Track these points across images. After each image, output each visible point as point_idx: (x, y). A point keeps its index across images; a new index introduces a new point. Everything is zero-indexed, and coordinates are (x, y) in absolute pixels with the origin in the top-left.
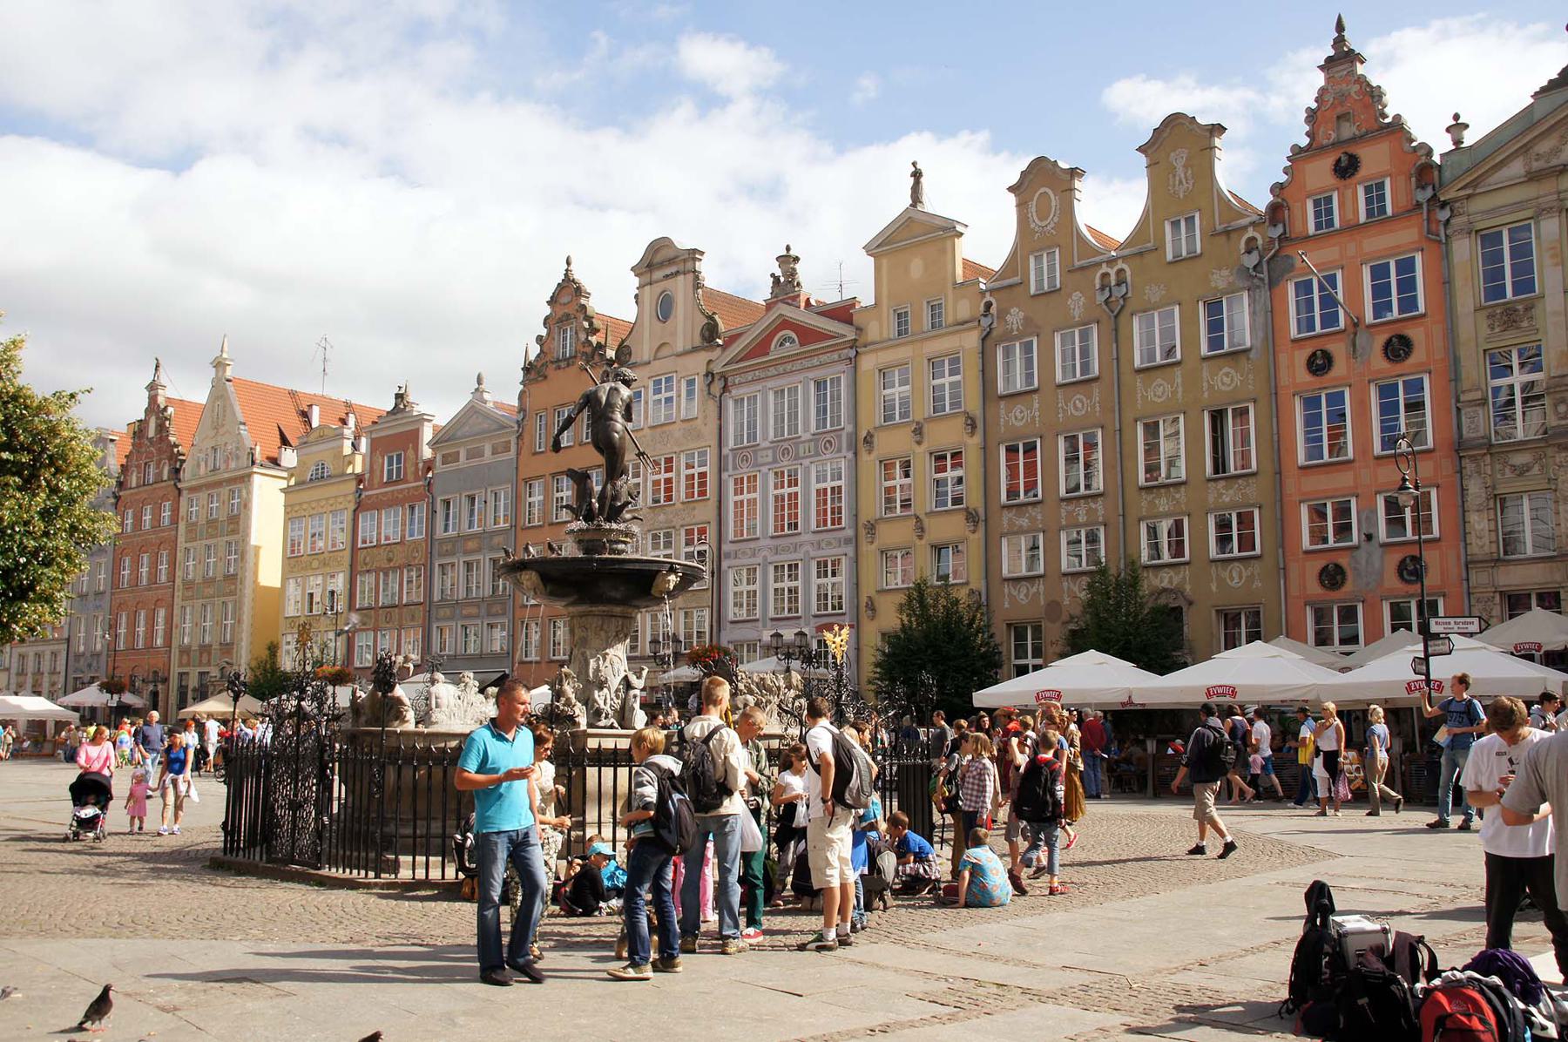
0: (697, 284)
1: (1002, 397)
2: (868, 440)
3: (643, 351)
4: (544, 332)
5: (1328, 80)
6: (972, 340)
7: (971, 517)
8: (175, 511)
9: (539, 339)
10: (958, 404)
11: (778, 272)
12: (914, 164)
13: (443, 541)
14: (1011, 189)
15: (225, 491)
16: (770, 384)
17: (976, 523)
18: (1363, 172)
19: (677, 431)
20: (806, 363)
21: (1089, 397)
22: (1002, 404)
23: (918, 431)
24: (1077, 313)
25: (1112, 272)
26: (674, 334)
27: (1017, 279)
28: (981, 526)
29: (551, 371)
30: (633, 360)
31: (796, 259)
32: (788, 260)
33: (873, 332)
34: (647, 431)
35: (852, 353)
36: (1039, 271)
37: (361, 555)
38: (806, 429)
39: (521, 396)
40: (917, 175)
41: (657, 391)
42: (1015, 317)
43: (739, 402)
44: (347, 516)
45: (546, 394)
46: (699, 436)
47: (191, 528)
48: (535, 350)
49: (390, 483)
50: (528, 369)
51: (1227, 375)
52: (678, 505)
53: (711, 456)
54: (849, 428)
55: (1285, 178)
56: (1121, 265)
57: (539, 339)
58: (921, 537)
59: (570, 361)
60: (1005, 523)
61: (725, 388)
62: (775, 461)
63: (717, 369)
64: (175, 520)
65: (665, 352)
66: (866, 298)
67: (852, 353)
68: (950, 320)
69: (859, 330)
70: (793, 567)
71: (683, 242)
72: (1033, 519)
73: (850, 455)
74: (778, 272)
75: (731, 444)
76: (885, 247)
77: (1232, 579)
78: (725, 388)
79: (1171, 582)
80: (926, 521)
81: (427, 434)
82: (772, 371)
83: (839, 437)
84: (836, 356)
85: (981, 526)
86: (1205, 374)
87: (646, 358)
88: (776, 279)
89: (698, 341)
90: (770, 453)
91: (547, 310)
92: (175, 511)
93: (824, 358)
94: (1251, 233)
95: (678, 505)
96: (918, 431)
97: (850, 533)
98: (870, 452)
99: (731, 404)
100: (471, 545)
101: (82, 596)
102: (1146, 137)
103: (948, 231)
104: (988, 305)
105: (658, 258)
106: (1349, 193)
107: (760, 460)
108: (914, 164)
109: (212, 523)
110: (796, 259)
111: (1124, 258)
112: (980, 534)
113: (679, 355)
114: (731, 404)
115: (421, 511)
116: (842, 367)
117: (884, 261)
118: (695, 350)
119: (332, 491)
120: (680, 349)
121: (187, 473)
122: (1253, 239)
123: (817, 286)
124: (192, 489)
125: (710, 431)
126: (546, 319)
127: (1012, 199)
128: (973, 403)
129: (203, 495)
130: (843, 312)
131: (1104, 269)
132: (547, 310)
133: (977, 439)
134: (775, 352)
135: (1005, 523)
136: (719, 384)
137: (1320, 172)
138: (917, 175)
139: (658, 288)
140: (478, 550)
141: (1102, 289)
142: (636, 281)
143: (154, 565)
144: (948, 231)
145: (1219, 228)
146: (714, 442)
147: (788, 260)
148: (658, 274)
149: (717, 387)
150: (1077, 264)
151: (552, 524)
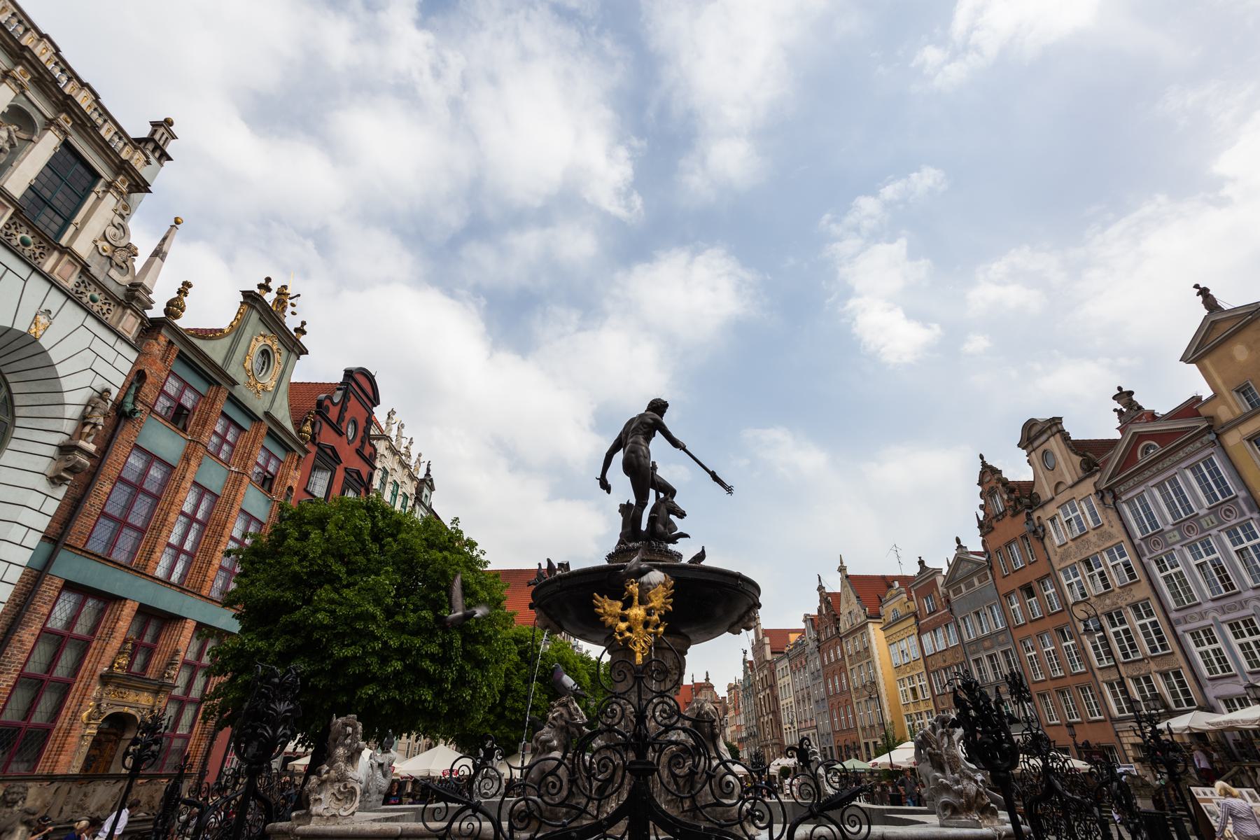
0: (1066, 437)
3: (1046, 491)
4: (982, 502)
8: (842, 649)
9: (981, 507)
11: (1119, 407)
15: (859, 635)
16: (1150, 483)
19: (1092, 537)
20: (1174, 458)
26: (1062, 474)
29: (994, 523)
30: (1043, 499)
32: (1124, 396)
34: (1070, 543)
37: (929, 660)
38: (1201, 506)
39: (983, 542)
41: (1066, 514)
43: (1129, 502)
45: (997, 540)
46: (1111, 536)
48: (981, 514)
49: (931, 613)
52: (1117, 590)
53: (1127, 548)
57: (981, 507)
59: (1003, 514)
61: (1115, 498)
62: (1183, 538)
63: (1103, 486)
65: (1062, 488)
71: (1043, 415)
74: (1119, 407)
75: (1139, 535)
78: (1115, 498)
81: (940, 580)
82: (1147, 474)
83: (1237, 504)
87: (1050, 496)
88: (1120, 412)
89: (1081, 474)
90: (1176, 533)
91: (980, 489)
92: (842, 649)
93: (1188, 449)
95: (1117, 590)
99: (1125, 507)
100: (987, 644)
105: (1033, 433)
107: (1170, 541)
113: (1072, 487)
114: (1125, 507)
115: (952, 629)
118: (1080, 481)
119: (904, 625)
120: (1070, 482)
121: (842, 630)
124: (846, 636)
125: (1117, 531)
126: (981, 495)
129: (851, 639)
130: (1191, 408)
132: (980, 489)
134: (1142, 459)
136: (1109, 495)
139: (1040, 451)
140: (992, 647)
142: (1025, 452)
143: (840, 680)
146: (1124, 537)
147: (1124, 396)
148: (1036, 444)
151: (1032, 621)
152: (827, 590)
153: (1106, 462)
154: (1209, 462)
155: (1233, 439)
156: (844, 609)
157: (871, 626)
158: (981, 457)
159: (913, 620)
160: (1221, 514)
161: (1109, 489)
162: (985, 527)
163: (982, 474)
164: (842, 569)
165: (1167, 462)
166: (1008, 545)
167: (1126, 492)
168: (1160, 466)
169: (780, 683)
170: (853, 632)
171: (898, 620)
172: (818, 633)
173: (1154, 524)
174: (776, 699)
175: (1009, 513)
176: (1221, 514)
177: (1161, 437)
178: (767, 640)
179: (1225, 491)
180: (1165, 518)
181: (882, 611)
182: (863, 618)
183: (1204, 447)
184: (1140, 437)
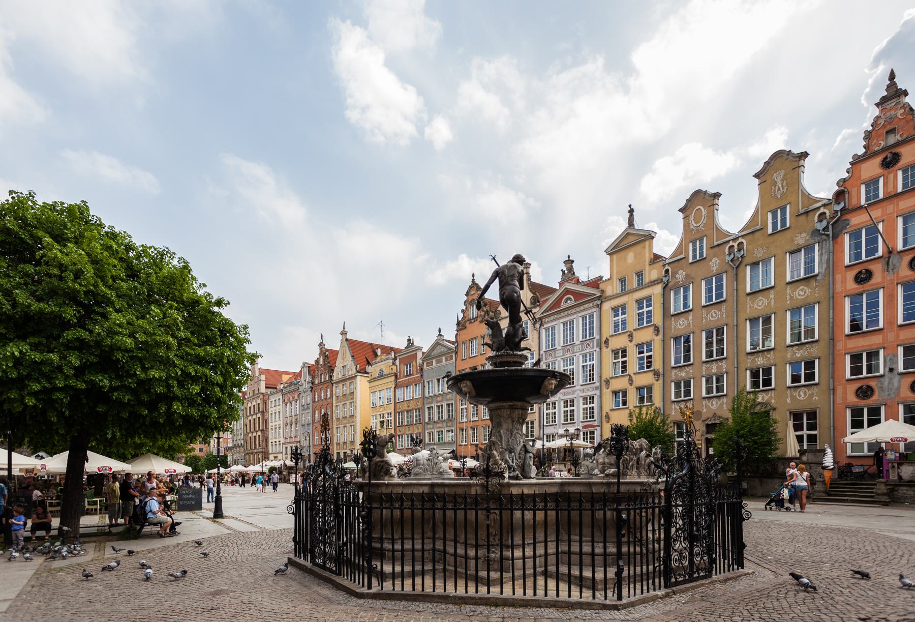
1: (673, 315)
2: (607, 342)
5: (881, 111)
6: (658, 289)
7: (656, 374)
8: (331, 392)
9: (463, 311)
10: (651, 321)
11: (565, 269)
12: (630, 206)
13: (428, 398)
14: (681, 210)
15: (348, 383)
17: (659, 376)
18: (903, 162)
20: (578, 309)
21: (720, 310)
22: (673, 319)
23: (631, 336)
24: (714, 269)
25: (736, 245)
27: (683, 256)
28: (661, 377)
29: (467, 325)
31: (573, 262)
33: (609, 291)
35: (599, 302)
36: (694, 250)
37: (398, 405)
40: (631, 211)
42: (681, 275)
43: (547, 329)
44: (393, 389)
45: (466, 335)
47: (337, 397)
48: (461, 316)
50: (458, 324)
51: (802, 290)
54: (598, 337)
55: (847, 175)
56: (740, 240)
57: (463, 311)
58: (631, 385)
60: (673, 374)
61: (541, 325)
64: (331, 397)
66: (606, 276)
67: (599, 302)
68: (647, 281)
69: (603, 291)
70: (572, 401)
72: (687, 373)
73: (598, 349)
74: (565, 269)
76: (615, 250)
79: (763, 398)
80: (634, 377)
81: (420, 355)
82: (562, 314)
84: (591, 305)
85: (661, 377)
86: (788, 291)
91: (465, 298)
92: (331, 392)
93: (586, 306)
94: (822, 210)
96: (631, 336)
97: (598, 384)
98: (607, 347)
100: (439, 399)
101: (303, 425)
102: (759, 167)
103: (649, 237)
104: (667, 271)
106: (891, 176)
108: (630, 206)
109: (344, 395)
110: (573, 262)
111: (742, 236)
112: (661, 381)
114: (544, 331)
115: (419, 387)
116: (595, 309)
117: (615, 257)
122: (824, 213)
123: (583, 274)
127: (681, 215)
128: (657, 319)
129: (341, 385)
130: (595, 283)
131: (731, 243)
132: (465, 298)
133: (660, 337)
134: (563, 305)
135: (673, 374)
137: (872, 168)
138: (631, 211)
141: (730, 254)
144: (649, 237)
145: (801, 211)
149: (537, 325)
150: (716, 243)
152: (326, 347)
153: (544, 302)
154: (591, 316)
156: (339, 363)
157: (358, 378)
158: (473, 276)
159: (393, 378)
160: (584, 346)
161: (540, 319)
162: (461, 326)
163: (471, 288)
164: (343, 333)
165: (574, 311)
166: (471, 340)
167: (548, 322)
168: (569, 312)
169: (271, 410)
170: (343, 381)
171: (382, 376)
172: (313, 378)
173: (554, 345)
174: (266, 422)
175: (479, 319)
176: (584, 346)
177: (578, 295)
178: (263, 377)
179: (591, 334)
180: (560, 342)
181: (369, 369)
182: (354, 371)
183: (593, 307)
184: (568, 291)
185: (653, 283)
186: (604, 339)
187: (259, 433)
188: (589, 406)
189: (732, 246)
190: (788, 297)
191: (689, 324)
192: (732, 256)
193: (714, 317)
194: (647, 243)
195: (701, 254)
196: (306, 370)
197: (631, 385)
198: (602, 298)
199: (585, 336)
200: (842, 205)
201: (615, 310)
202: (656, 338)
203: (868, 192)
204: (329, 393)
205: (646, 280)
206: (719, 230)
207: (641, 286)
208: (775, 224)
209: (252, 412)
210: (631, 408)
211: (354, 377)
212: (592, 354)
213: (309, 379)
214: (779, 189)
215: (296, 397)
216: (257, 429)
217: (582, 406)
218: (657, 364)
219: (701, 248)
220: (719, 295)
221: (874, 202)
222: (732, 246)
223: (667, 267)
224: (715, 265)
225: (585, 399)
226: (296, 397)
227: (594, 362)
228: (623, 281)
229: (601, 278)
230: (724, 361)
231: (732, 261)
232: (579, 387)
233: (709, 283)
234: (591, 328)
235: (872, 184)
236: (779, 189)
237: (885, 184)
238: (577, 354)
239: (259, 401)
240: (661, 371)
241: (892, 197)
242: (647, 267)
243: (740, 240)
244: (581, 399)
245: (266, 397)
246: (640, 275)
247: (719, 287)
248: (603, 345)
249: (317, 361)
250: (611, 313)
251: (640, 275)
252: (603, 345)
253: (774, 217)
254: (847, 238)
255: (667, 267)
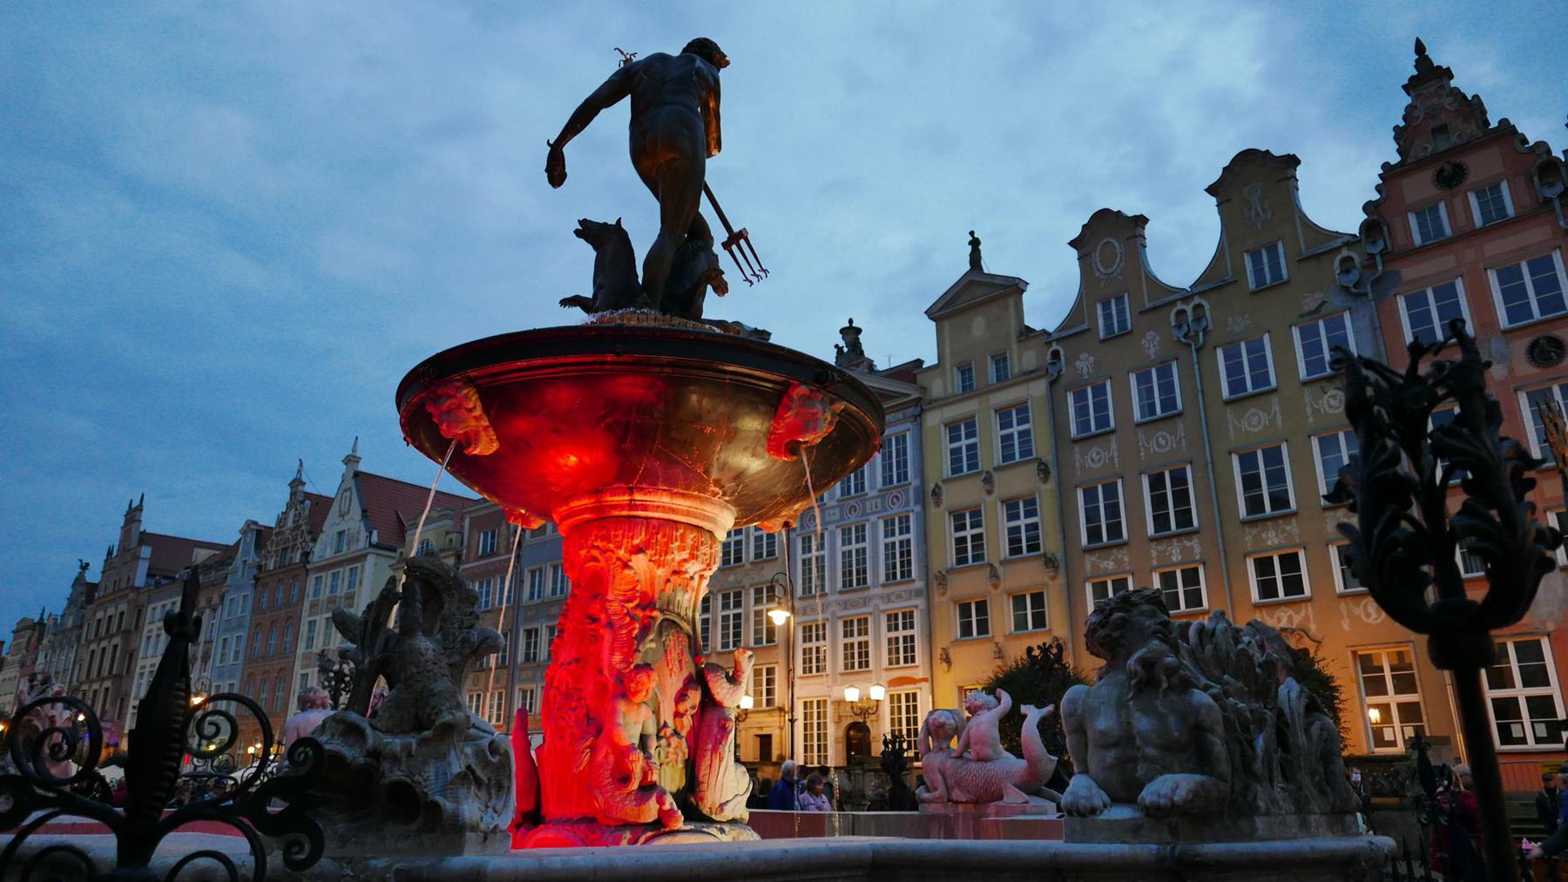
1: (1075, 441)
2: (936, 493)
5: (1415, 98)
6: (1039, 389)
7: (1050, 562)
10: (1029, 452)
17: (1056, 568)
18: (1473, 178)
22: (1077, 448)
23: (988, 480)
24: (1152, 351)
25: (1189, 308)
27: (1085, 327)
28: (1062, 571)
33: (937, 389)
36: (1108, 317)
56: (1197, 300)
58: (995, 586)
60: (1088, 566)
66: (930, 359)
68: (1016, 371)
69: (924, 389)
70: (863, 622)
72: (1118, 562)
73: (918, 508)
77: (1368, 615)
80: (1000, 570)
84: (900, 415)
85: (1062, 571)
86: (1307, 399)
96: (988, 480)
97: (919, 584)
98: (938, 504)
103: (1015, 287)
104: (1056, 354)
106: (1458, 201)
111: (1200, 294)
112: (1061, 579)
116: (908, 425)
117: (946, 324)
122: (1350, 259)
127: (1074, 253)
128: (1042, 447)
131: (1180, 306)
133: (1051, 485)
135: (1088, 566)
137: (1421, 186)
141: (1179, 326)
144: (1015, 287)
145: (1305, 253)
150: (1148, 305)
155: (933, 419)
157: (371, 559)
178: (146, 551)
179: (903, 476)
182: (362, 543)
183: (905, 419)
185: (1029, 376)
186: (932, 486)
187: (108, 684)
188: (901, 633)
189: (1182, 312)
190: (1309, 410)
191: (1112, 459)
192: (1185, 329)
193: (1163, 445)
194: (1011, 301)
195: (1122, 322)
196: (251, 539)
197: (995, 586)
198: (921, 406)
199: (888, 479)
200: (1380, 245)
201: (953, 429)
202: (1044, 487)
203: (1422, 225)
204: (296, 592)
205: (1014, 367)
206: (1154, 282)
207: (1004, 379)
208: (1258, 272)
209: (103, 632)
210: (1000, 639)
211: (361, 558)
212: (905, 520)
213: (252, 558)
214: (1257, 214)
215: (216, 599)
216: (105, 672)
217: (885, 635)
218: (1050, 542)
219: (1121, 312)
220: (1169, 403)
221: (1436, 245)
222: (1182, 312)
223: (1055, 346)
224: (1151, 344)
225: (892, 618)
226: (216, 599)
227: (912, 536)
228: (965, 371)
229: (919, 362)
230: (1195, 540)
231: (1185, 336)
232: (879, 591)
233: (1144, 379)
234: (902, 464)
235: (1426, 212)
236: (1257, 214)
237: (1451, 214)
238: (873, 518)
239: (123, 607)
240: (1059, 556)
241: (1467, 235)
242: (1015, 346)
243: (1197, 300)
244: (884, 618)
245: (143, 598)
246: (1000, 360)
247: (1167, 388)
248: (930, 500)
249: (281, 520)
250: (945, 435)
251: (1000, 360)
252: (930, 500)
253: (1257, 262)
254: (1401, 303)
255: (1055, 346)
